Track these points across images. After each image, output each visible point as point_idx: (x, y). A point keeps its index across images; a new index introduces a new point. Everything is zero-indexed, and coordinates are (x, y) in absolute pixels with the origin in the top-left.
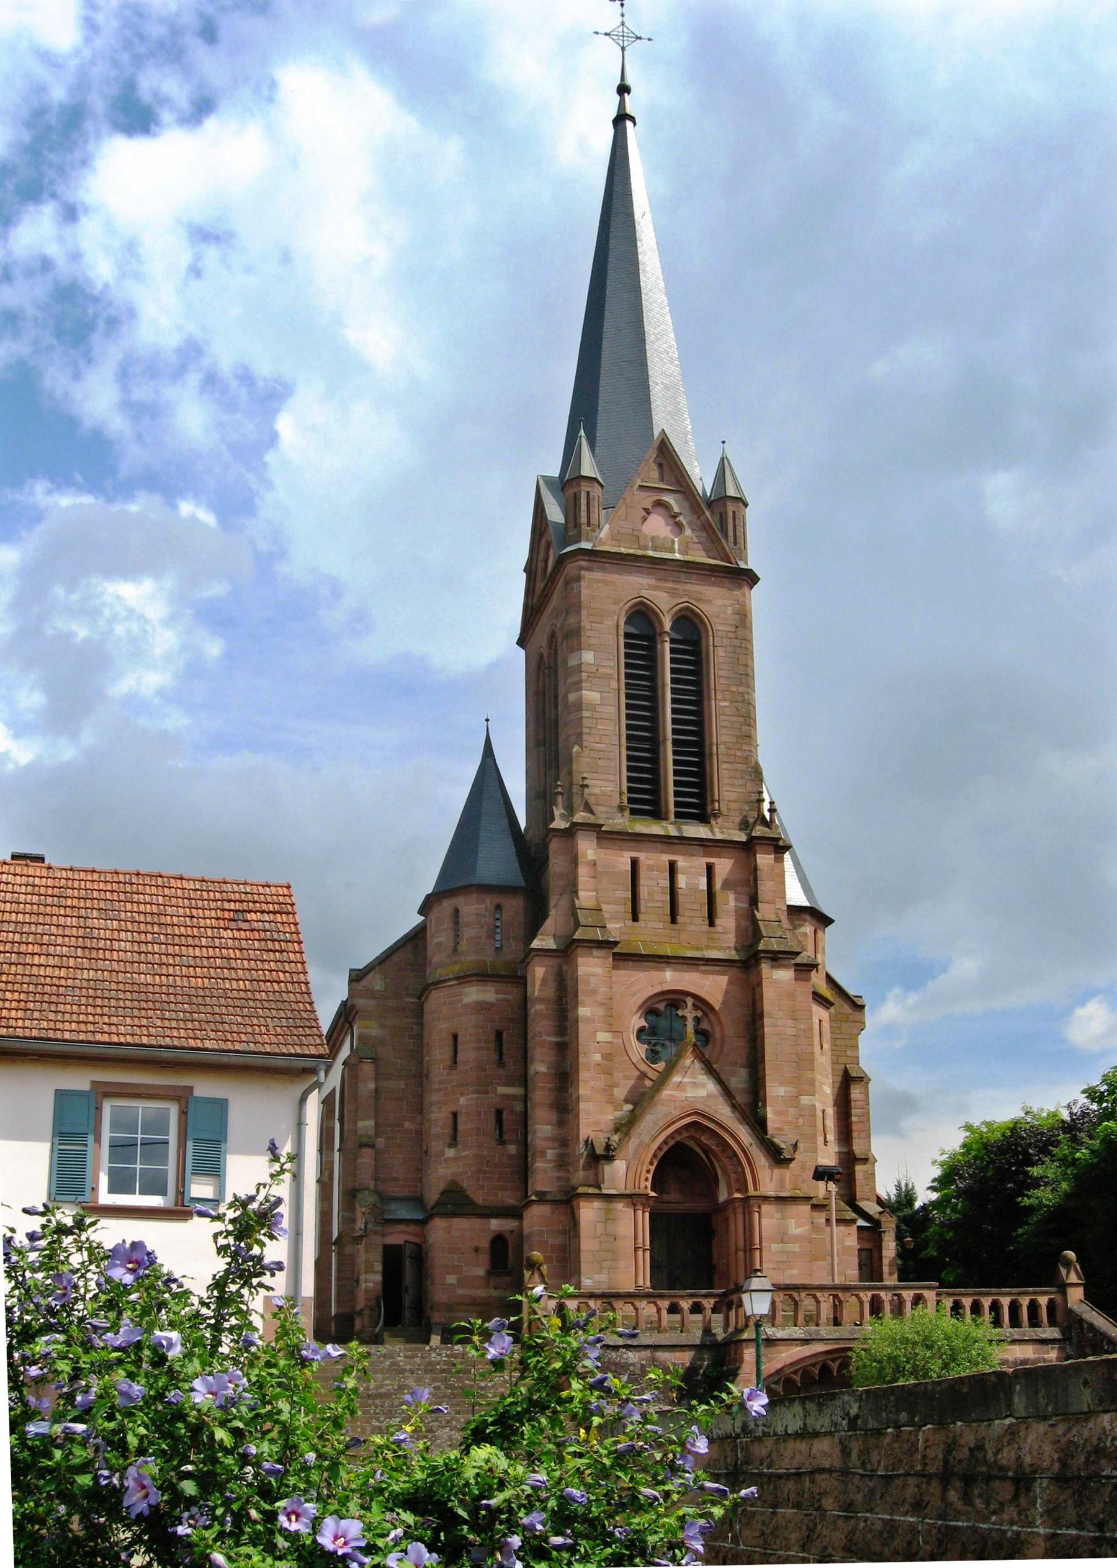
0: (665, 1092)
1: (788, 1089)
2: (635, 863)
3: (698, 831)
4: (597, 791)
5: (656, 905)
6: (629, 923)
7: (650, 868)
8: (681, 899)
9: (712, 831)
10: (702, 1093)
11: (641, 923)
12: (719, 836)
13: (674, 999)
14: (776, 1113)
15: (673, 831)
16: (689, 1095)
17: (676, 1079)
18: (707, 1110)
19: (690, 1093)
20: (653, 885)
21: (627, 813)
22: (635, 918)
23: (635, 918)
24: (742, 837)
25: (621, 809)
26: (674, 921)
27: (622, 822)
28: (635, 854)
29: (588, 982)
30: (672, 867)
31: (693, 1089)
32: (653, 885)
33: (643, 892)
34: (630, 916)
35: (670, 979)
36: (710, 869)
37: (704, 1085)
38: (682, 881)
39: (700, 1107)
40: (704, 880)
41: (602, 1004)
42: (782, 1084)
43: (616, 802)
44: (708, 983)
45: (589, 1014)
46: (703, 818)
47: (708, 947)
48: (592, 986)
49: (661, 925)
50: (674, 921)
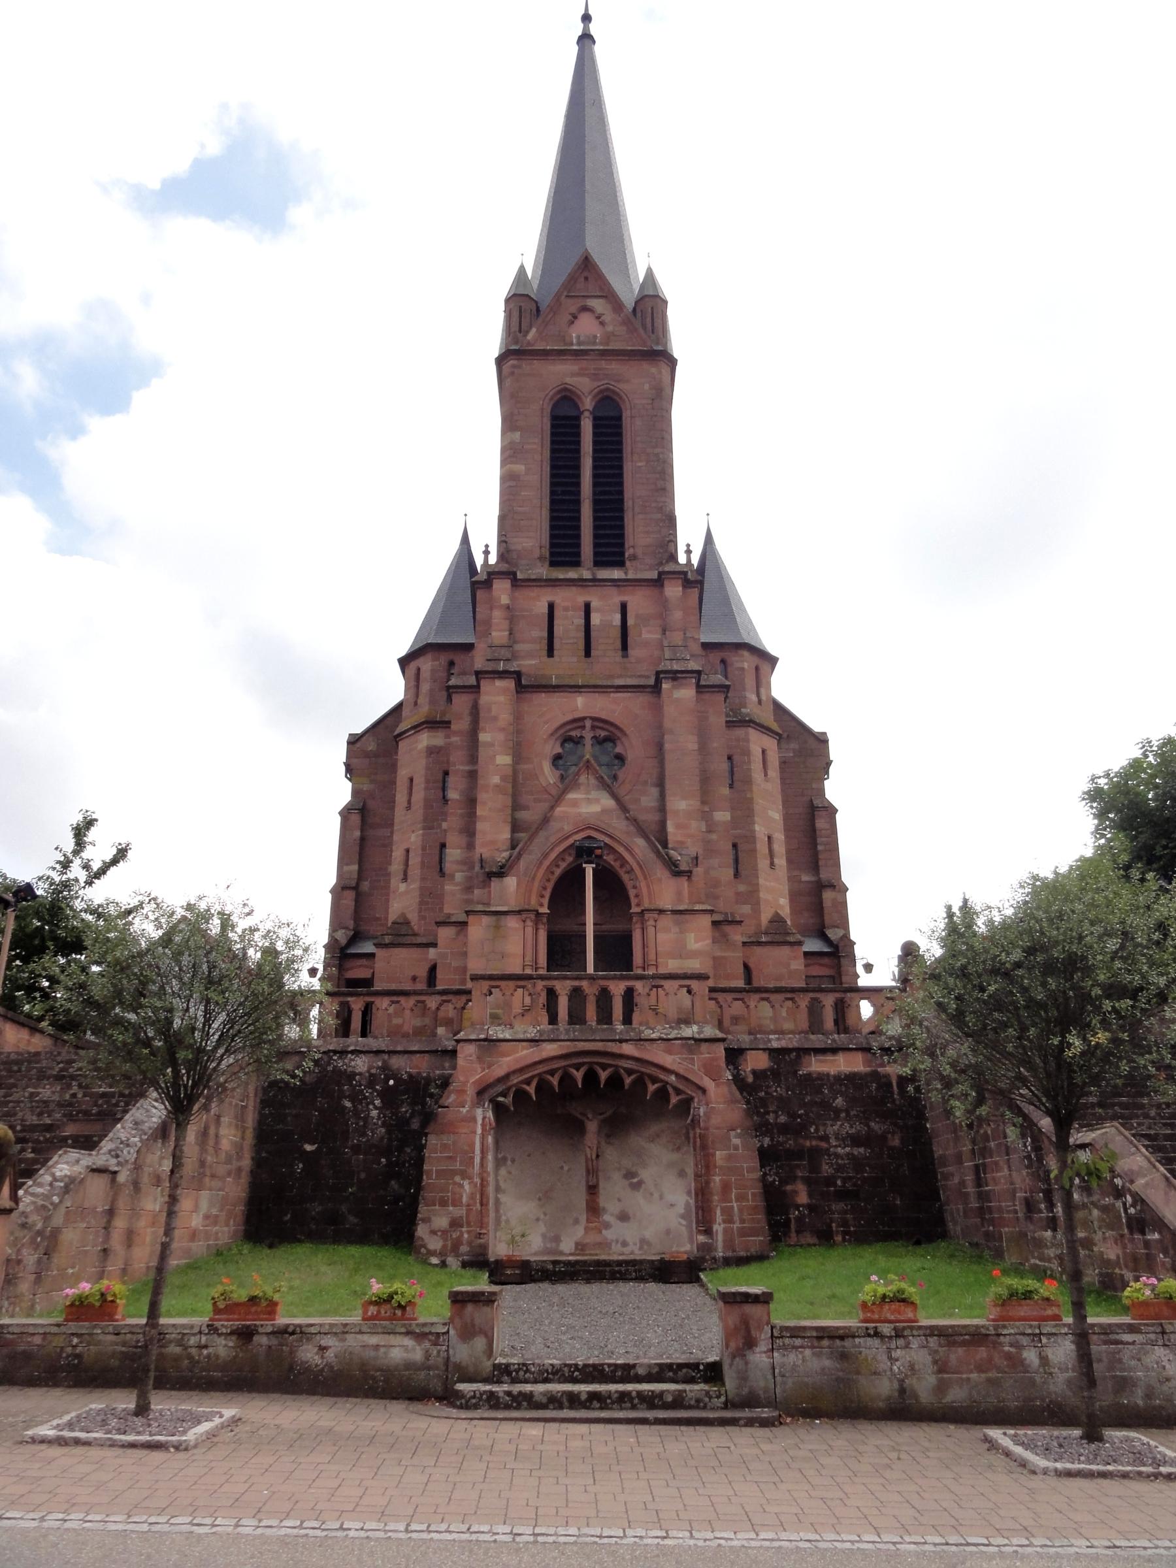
0: (558, 809)
1: (692, 802)
2: (551, 607)
3: (616, 574)
4: (519, 547)
6: (545, 659)
7: (566, 609)
8: (592, 634)
9: (626, 573)
10: (596, 808)
11: (556, 658)
12: (630, 576)
13: (578, 722)
14: (678, 826)
15: (587, 575)
16: (584, 810)
17: (571, 796)
20: (568, 626)
21: (547, 563)
22: (550, 652)
23: (550, 652)
24: (654, 575)
25: (541, 558)
26: (588, 653)
27: (543, 571)
28: (550, 599)
29: (489, 710)
30: (587, 608)
31: (588, 805)
32: (568, 626)
33: (558, 630)
34: (545, 653)
35: (581, 704)
36: (624, 608)
37: (597, 801)
38: (595, 619)
40: (618, 616)
43: (537, 554)
45: (489, 739)
46: (620, 564)
47: (620, 676)
48: (493, 713)
49: (575, 659)
50: (588, 653)
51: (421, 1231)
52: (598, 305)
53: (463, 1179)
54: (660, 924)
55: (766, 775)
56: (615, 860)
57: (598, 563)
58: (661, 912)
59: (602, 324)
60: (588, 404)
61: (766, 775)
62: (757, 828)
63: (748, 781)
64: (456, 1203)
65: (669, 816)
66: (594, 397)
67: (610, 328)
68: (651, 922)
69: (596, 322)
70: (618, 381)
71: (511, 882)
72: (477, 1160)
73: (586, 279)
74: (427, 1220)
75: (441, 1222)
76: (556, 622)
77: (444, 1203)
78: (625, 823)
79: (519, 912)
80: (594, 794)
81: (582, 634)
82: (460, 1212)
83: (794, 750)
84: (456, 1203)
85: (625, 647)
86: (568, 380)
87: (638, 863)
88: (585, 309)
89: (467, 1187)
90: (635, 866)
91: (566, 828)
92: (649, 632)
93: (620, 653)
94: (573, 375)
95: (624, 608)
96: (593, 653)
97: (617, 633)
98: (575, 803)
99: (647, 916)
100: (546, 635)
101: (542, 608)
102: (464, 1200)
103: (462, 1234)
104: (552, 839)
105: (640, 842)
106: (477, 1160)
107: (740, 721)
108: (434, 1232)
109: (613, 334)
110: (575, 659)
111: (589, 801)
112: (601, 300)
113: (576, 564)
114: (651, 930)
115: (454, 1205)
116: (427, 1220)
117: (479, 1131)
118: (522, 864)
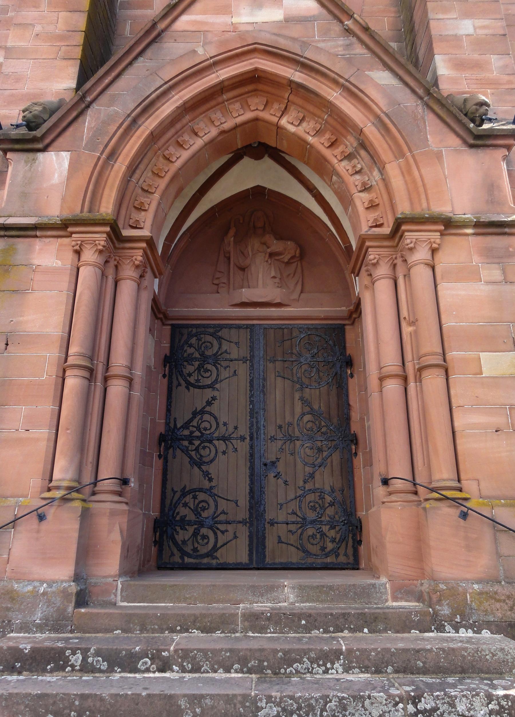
0: (185, 18)
14: (460, 65)
18: (283, 43)
39: (266, 38)
42: (467, 15)
54: (445, 261)
56: (318, 133)
58: (449, 225)
68: (422, 254)
71: (56, 165)
78: (341, 41)
79: (63, 227)
90: (371, 132)
91: (200, 51)
99: (410, 237)
104: (169, 73)
105: (383, 77)
114: (421, 276)
118: (89, 122)
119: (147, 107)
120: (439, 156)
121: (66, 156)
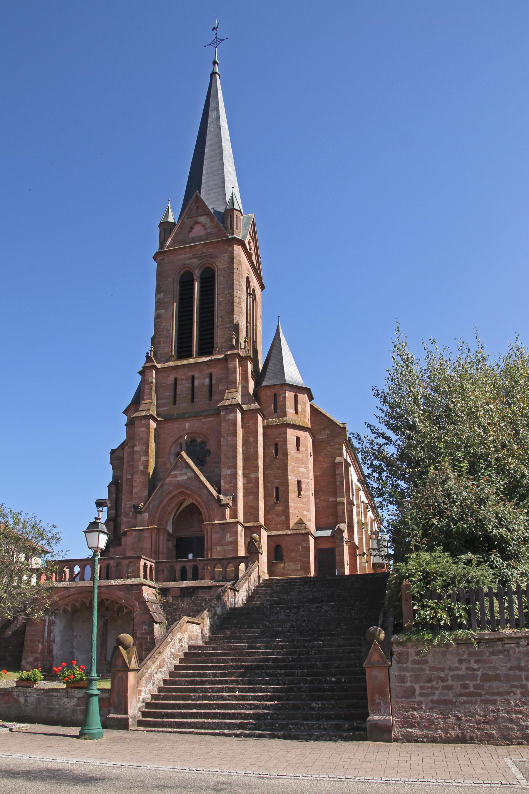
0: (167, 479)
2: (176, 380)
5: (185, 395)
7: (182, 380)
8: (195, 391)
10: (185, 477)
11: (177, 405)
19: (180, 478)
26: (192, 401)
30: (193, 378)
32: (183, 388)
37: (186, 474)
38: (197, 383)
41: (144, 444)
44: (206, 427)
46: (209, 353)
49: (186, 405)
50: (192, 401)
51: (24, 662)
52: (202, 219)
53: (39, 643)
55: (298, 450)
57: (201, 354)
59: (206, 229)
60: (197, 273)
61: (298, 450)
62: (290, 477)
63: (285, 454)
64: (36, 652)
65: (222, 477)
66: (200, 268)
67: (209, 231)
69: (203, 228)
70: (211, 258)
72: (46, 636)
73: (198, 207)
74: (26, 659)
75: (31, 659)
76: (178, 387)
77: (32, 652)
80: (184, 471)
81: (190, 391)
82: (38, 655)
83: (328, 435)
84: (36, 652)
85: (211, 395)
86: (187, 262)
87: (204, 503)
88: (197, 223)
89: (40, 646)
92: (223, 386)
93: (208, 399)
94: (190, 258)
95: (211, 375)
96: (195, 400)
97: (207, 389)
98: (175, 476)
100: (172, 394)
101: (171, 380)
102: (39, 651)
103: (38, 664)
106: (46, 636)
107: (281, 424)
108: (28, 663)
109: (210, 233)
110: (186, 405)
111: (182, 474)
112: (205, 217)
113: (190, 356)
115: (35, 653)
116: (26, 659)
117: (47, 624)
119: (161, 502)
120: (214, 509)
121: (147, 514)
